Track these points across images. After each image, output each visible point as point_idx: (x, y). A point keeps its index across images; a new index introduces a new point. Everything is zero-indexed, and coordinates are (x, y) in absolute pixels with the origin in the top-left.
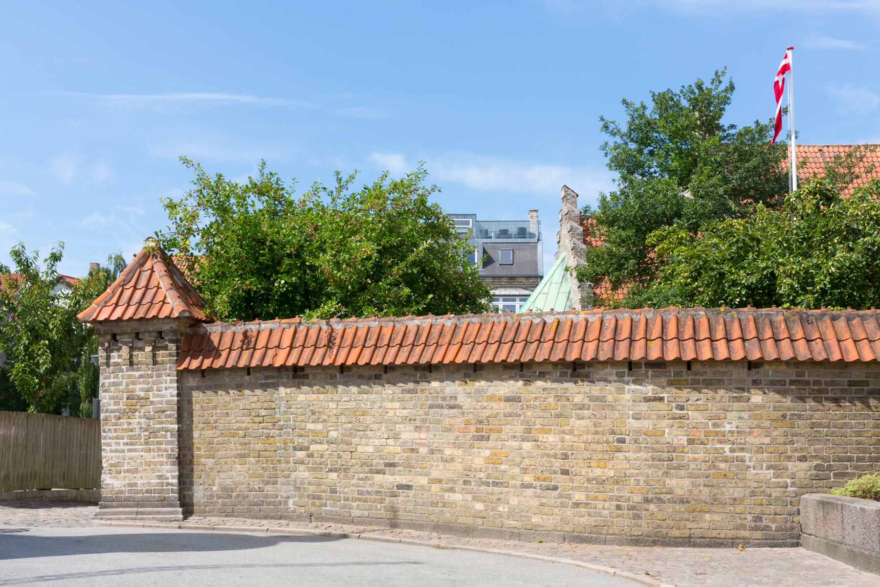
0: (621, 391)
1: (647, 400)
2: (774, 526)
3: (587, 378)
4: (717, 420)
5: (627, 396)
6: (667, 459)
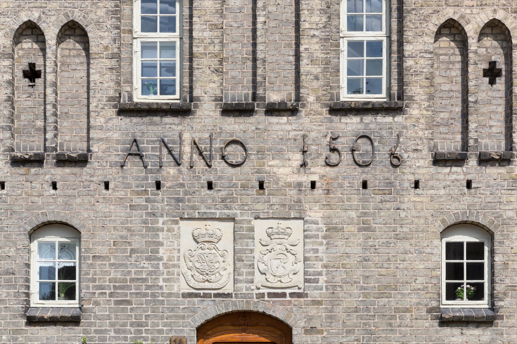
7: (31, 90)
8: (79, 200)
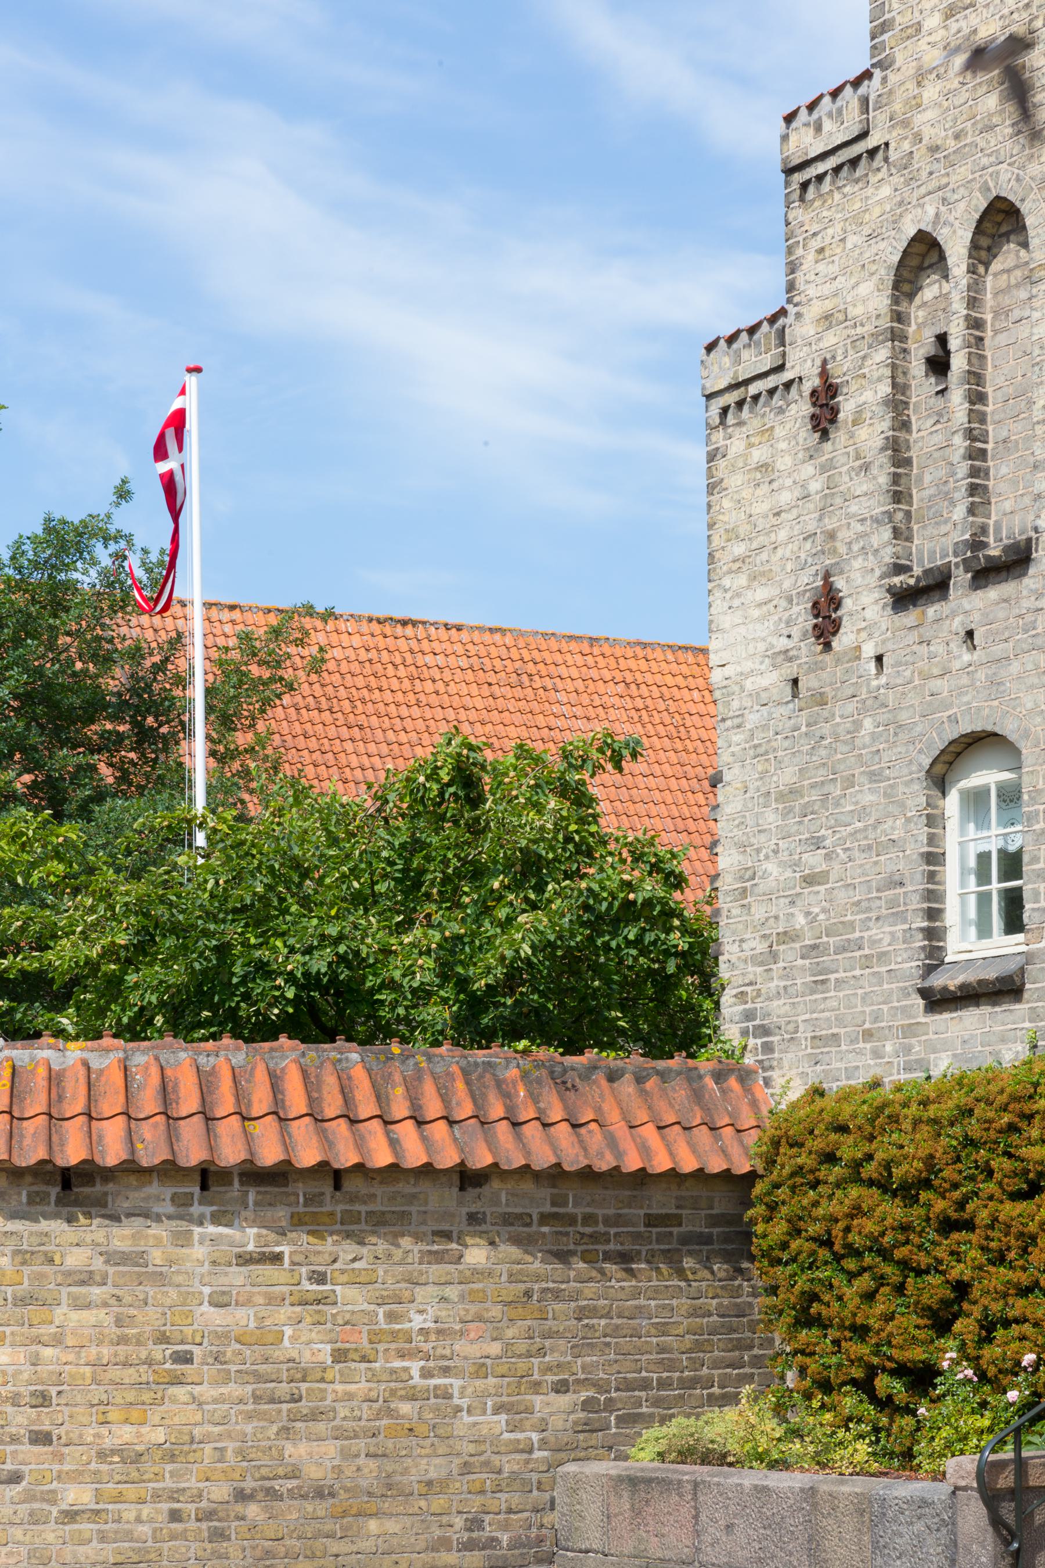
0: (183, 1239)
1: (245, 1260)
2: (505, 1538)
3: (101, 1208)
4: (394, 1303)
5: (199, 1251)
6: (286, 1395)
7: (940, 402)
8: (1015, 667)
